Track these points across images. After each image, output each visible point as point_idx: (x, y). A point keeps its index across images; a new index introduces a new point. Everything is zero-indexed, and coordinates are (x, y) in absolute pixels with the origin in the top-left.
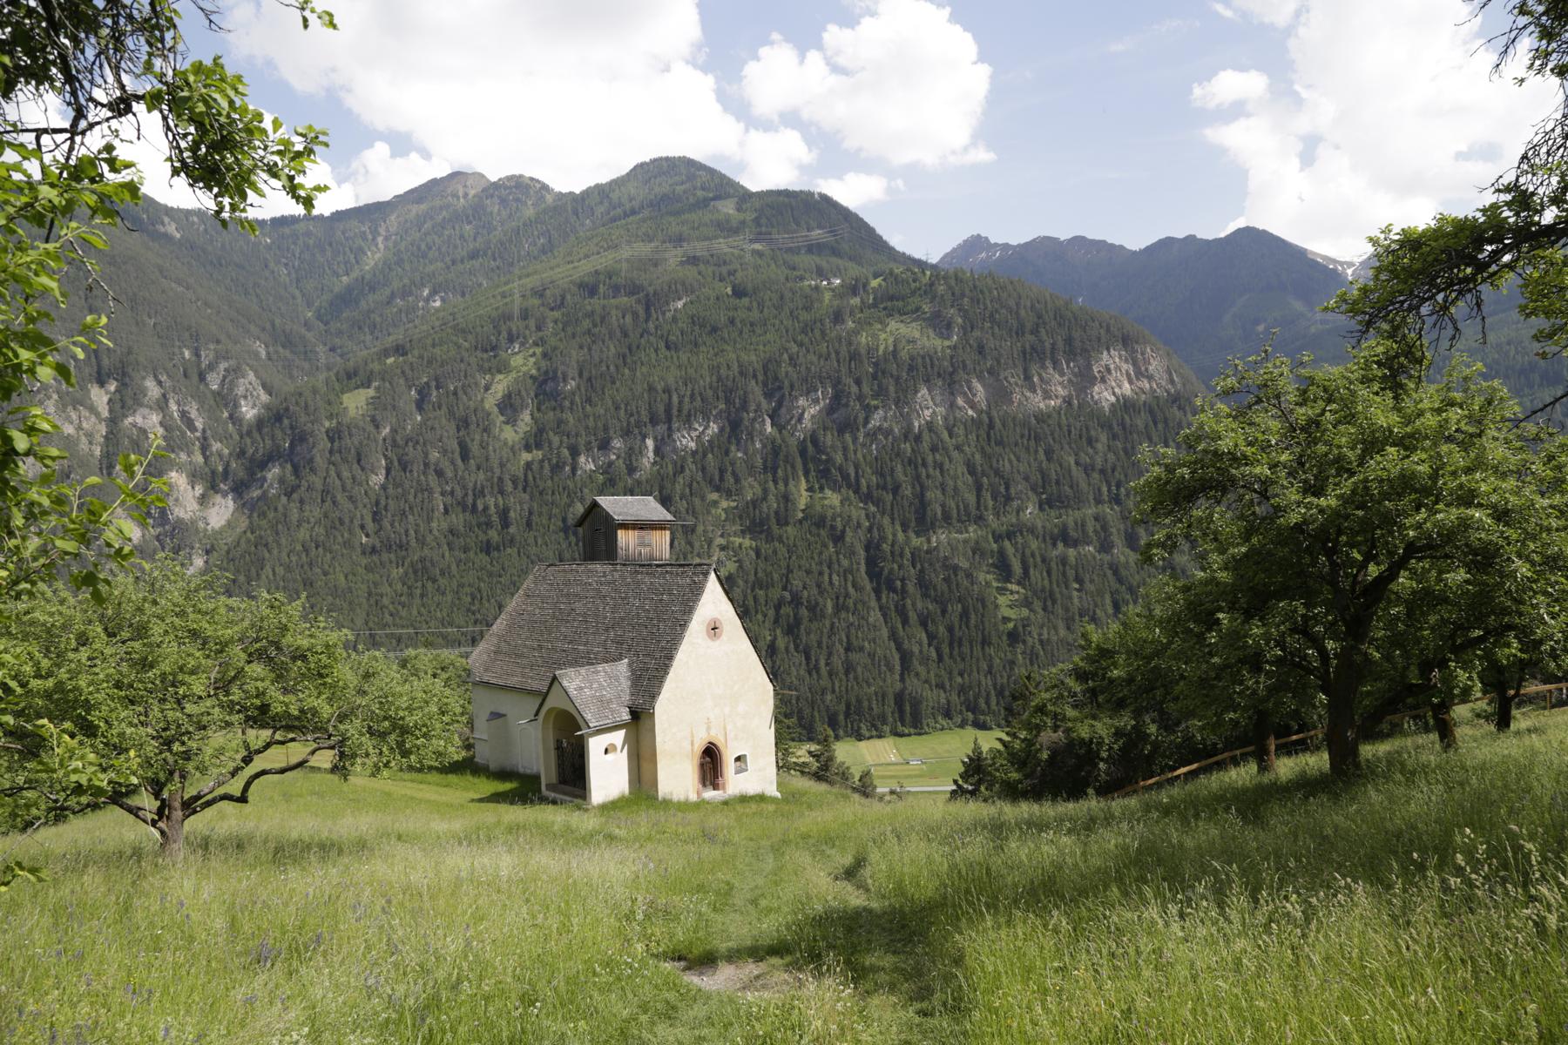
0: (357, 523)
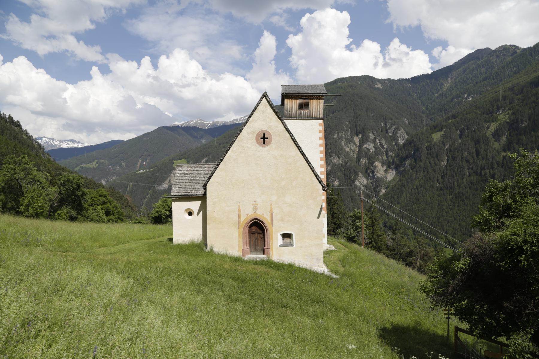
0: (435, 179)
